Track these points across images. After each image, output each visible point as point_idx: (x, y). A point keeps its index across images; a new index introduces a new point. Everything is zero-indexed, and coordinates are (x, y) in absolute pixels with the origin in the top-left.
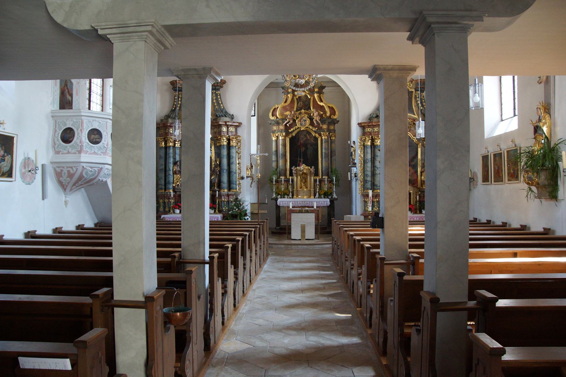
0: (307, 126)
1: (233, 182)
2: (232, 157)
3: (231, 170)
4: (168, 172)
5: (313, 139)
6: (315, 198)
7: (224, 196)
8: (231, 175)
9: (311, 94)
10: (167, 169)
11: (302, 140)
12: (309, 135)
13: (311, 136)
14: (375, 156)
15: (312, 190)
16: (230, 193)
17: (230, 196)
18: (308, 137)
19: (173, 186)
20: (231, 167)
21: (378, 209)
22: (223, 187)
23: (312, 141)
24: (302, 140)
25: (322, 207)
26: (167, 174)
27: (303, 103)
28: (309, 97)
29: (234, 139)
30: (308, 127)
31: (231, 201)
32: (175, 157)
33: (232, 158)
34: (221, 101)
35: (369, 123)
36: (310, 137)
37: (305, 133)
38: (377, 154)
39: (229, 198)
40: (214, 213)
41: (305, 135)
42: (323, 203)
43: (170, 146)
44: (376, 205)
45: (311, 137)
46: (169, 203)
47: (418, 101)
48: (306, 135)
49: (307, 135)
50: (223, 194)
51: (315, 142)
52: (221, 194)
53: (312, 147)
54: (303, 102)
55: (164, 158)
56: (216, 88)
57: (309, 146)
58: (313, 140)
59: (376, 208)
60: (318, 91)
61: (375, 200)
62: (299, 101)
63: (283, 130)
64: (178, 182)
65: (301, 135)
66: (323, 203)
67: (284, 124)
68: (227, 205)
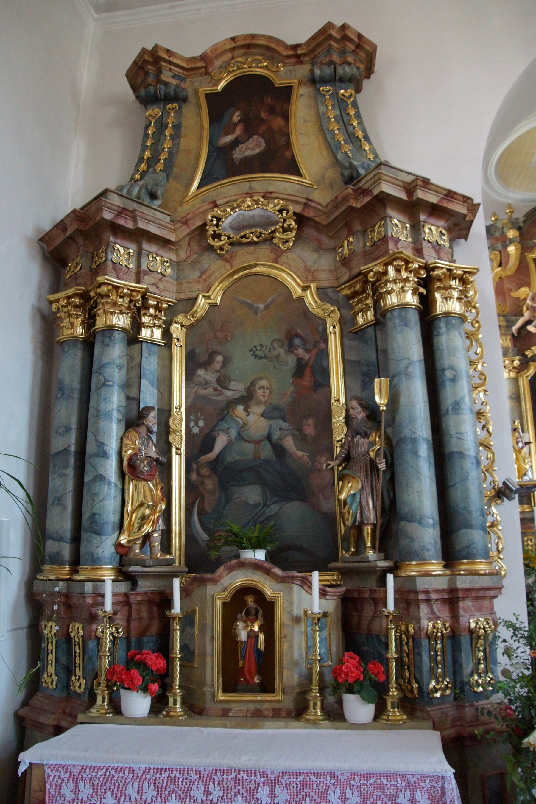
1: (470, 513)
2: (448, 374)
3: (453, 445)
4: (94, 467)
7: (428, 601)
8: (455, 477)
10: (91, 448)
16: (462, 583)
17: (464, 598)
19: (118, 545)
20: (453, 432)
22: (416, 546)
26: (87, 478)
29: (453, 283)
31: (471, 632)
32: (133, 393)
33: (454, 380)
34: (364, 131)
39: (455, 616)
40: (377, 717)
43: (111, 329)
46: (92, 645)
50: (427, 592)
52: (416, 592)
55: (76, 395)
56: (340, 71)
63: (510, 350)
64: (143, 518)
67: (515, 328)
68: (449, 658)
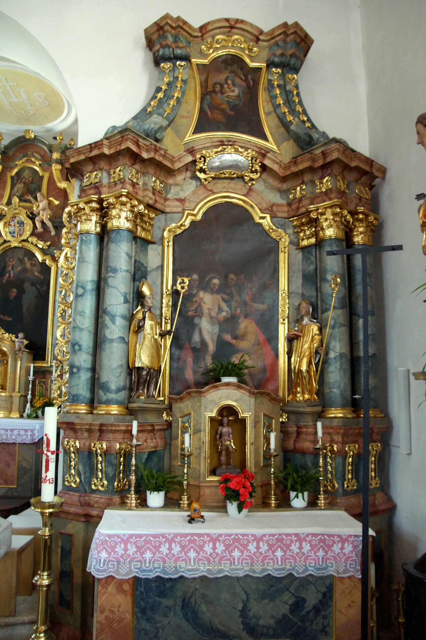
0: (24, 237)
5: (38, 268)
6: (22, 416)
9: (46, 166)
11: (12, 272)
12: (29, 259)
13: (34, 262)
14: (107, 272)
15: (16, 395)
18: (28, 265)
21: (106, 482)
23: (36, 274)
24: (12, 272)
25: (19, 443)
27: (24, 187)
28: (41, 175)
30: (26, 241)
35: (91, 151)
36: (31, 264)
37: (20, 254)
38: (111, 264)
41: (20, 260)
42: (22, 433)
44: (99, 466)
45: (35, 265)
47: (276, 97)
48: (23, 258)
49: (26, 259)
51: (42, 277)
53: (34, 288)
54: (25, 183)
57: (27, 286)
58: (38, 273)
59: (101, 480)
60: (61, 159)
61: (98, 446)
62: (16, 181)
65: (10, 258)
66: (22, 433)
